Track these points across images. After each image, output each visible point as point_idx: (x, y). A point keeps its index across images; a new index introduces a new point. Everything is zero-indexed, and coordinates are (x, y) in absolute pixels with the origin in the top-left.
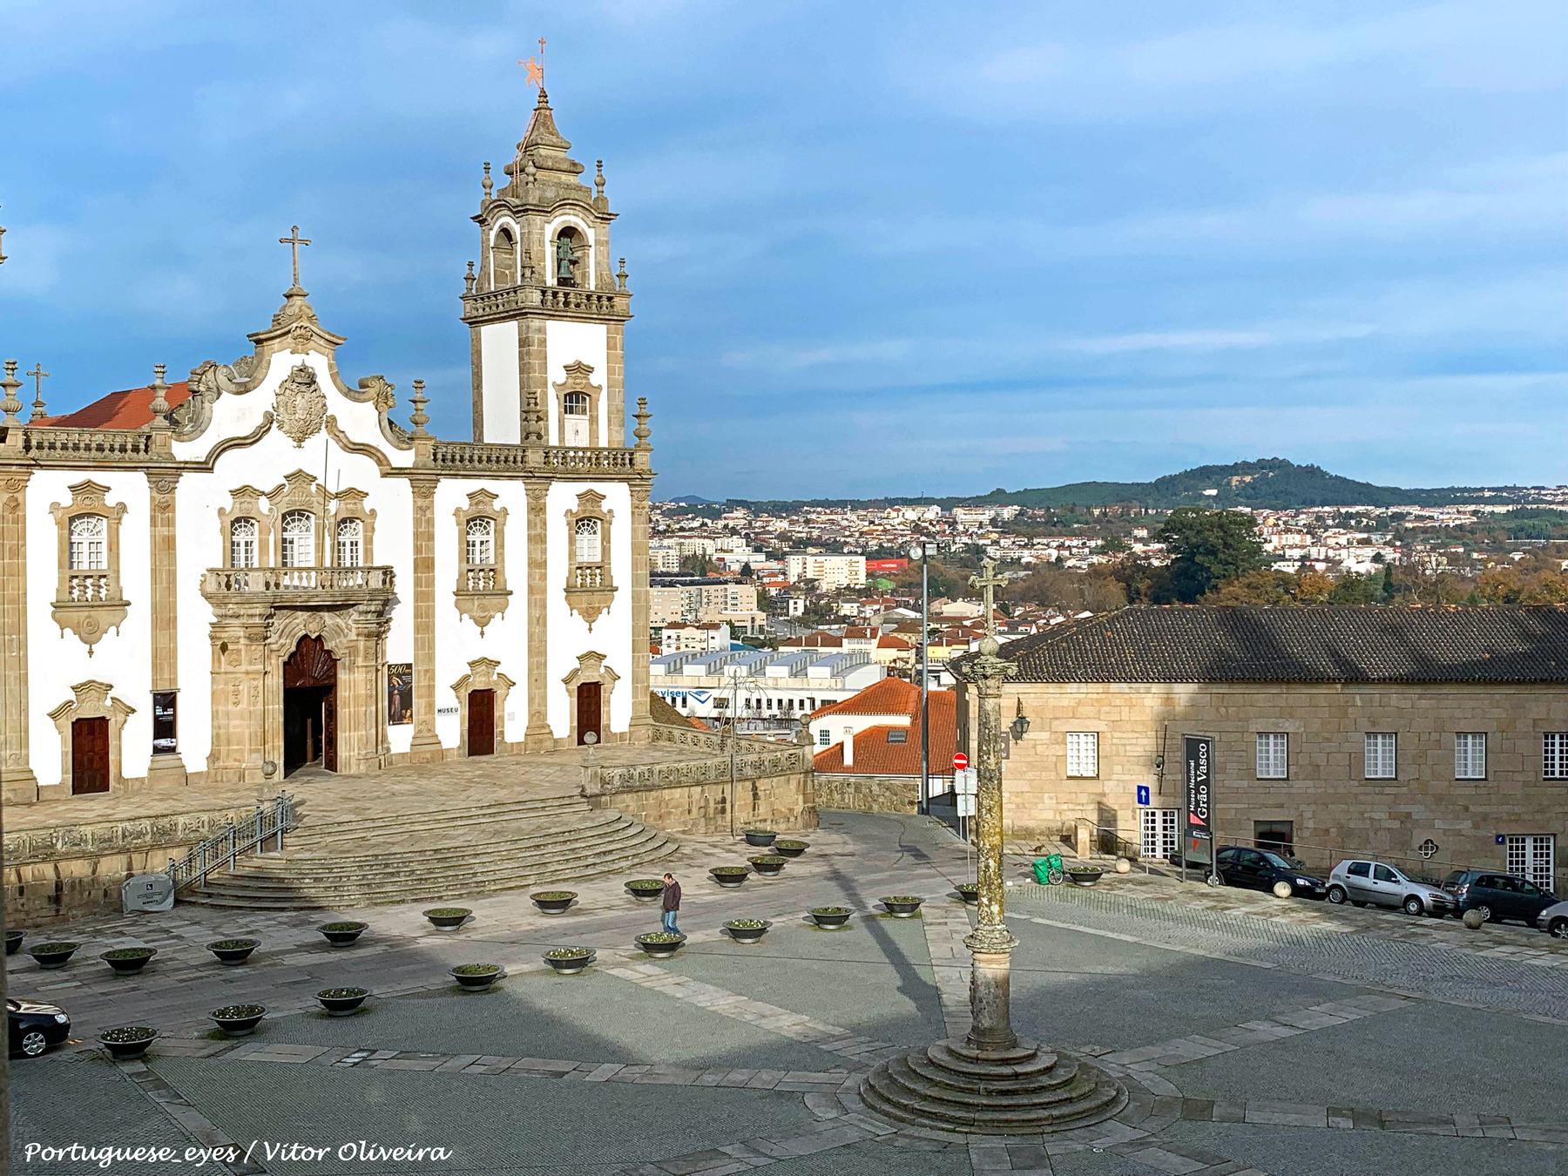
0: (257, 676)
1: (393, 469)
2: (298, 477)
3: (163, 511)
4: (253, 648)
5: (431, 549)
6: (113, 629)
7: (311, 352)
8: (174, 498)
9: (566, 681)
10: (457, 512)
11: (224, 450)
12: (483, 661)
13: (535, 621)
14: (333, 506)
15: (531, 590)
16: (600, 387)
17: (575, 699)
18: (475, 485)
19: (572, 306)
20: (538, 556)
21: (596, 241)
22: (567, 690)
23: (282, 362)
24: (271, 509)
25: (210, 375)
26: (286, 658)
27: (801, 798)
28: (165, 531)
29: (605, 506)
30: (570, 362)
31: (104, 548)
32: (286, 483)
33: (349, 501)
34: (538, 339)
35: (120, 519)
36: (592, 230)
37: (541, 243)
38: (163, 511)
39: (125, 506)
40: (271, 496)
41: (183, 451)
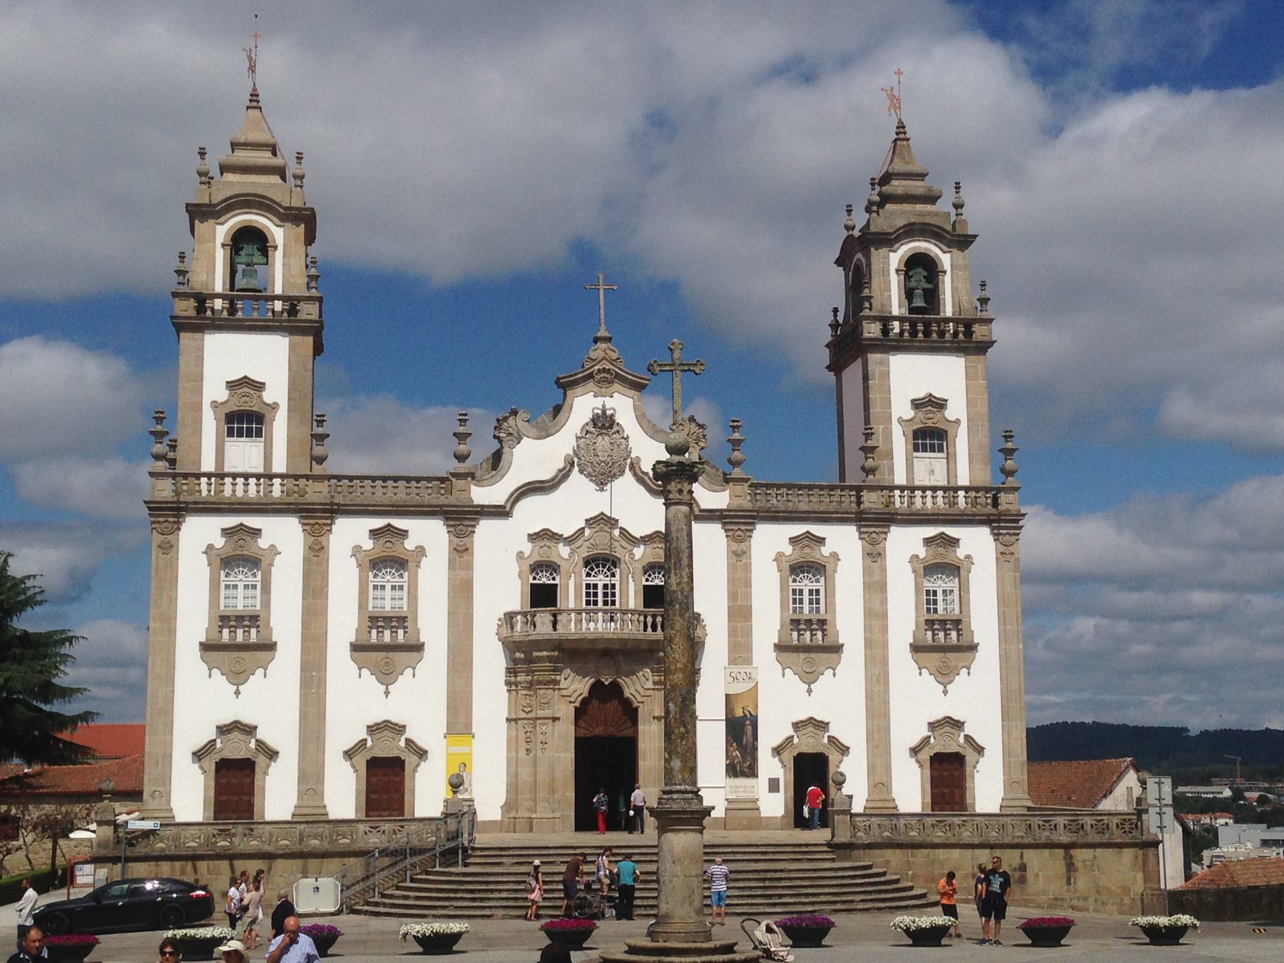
0: (546, 721)
2: (603, 521)
3: (461, 553)
5: (748, 596)
6: (409, 671)
7: (616, 395)
8: (472, 542)
9: (915, 751)
10: (779, 557)
12: (811, 721)
13: (874, 679)
14: (639, 552)
15: (868, 644)
16: (958, 422)
17: (928, 772)
18: (798, 529)
19: (934, 335)
20: (877, 607)
21: (952, 265)
22: (918, 761)
23: (584, 406)
24: (571, 554)
25: (511, 421)
26: (577, 704)
27: (1140, 876)
28: (463, 574)
29: (961, 553)
30: (920, 394)
31: (405, 593)
33: (655, 546)
34: (879, 372)
35: (419, 562)
36: (948, 255)
37: (886, 273)
38: (461, 553)
39: (424, 549)
40: (569, 540)
41: (481, 495)
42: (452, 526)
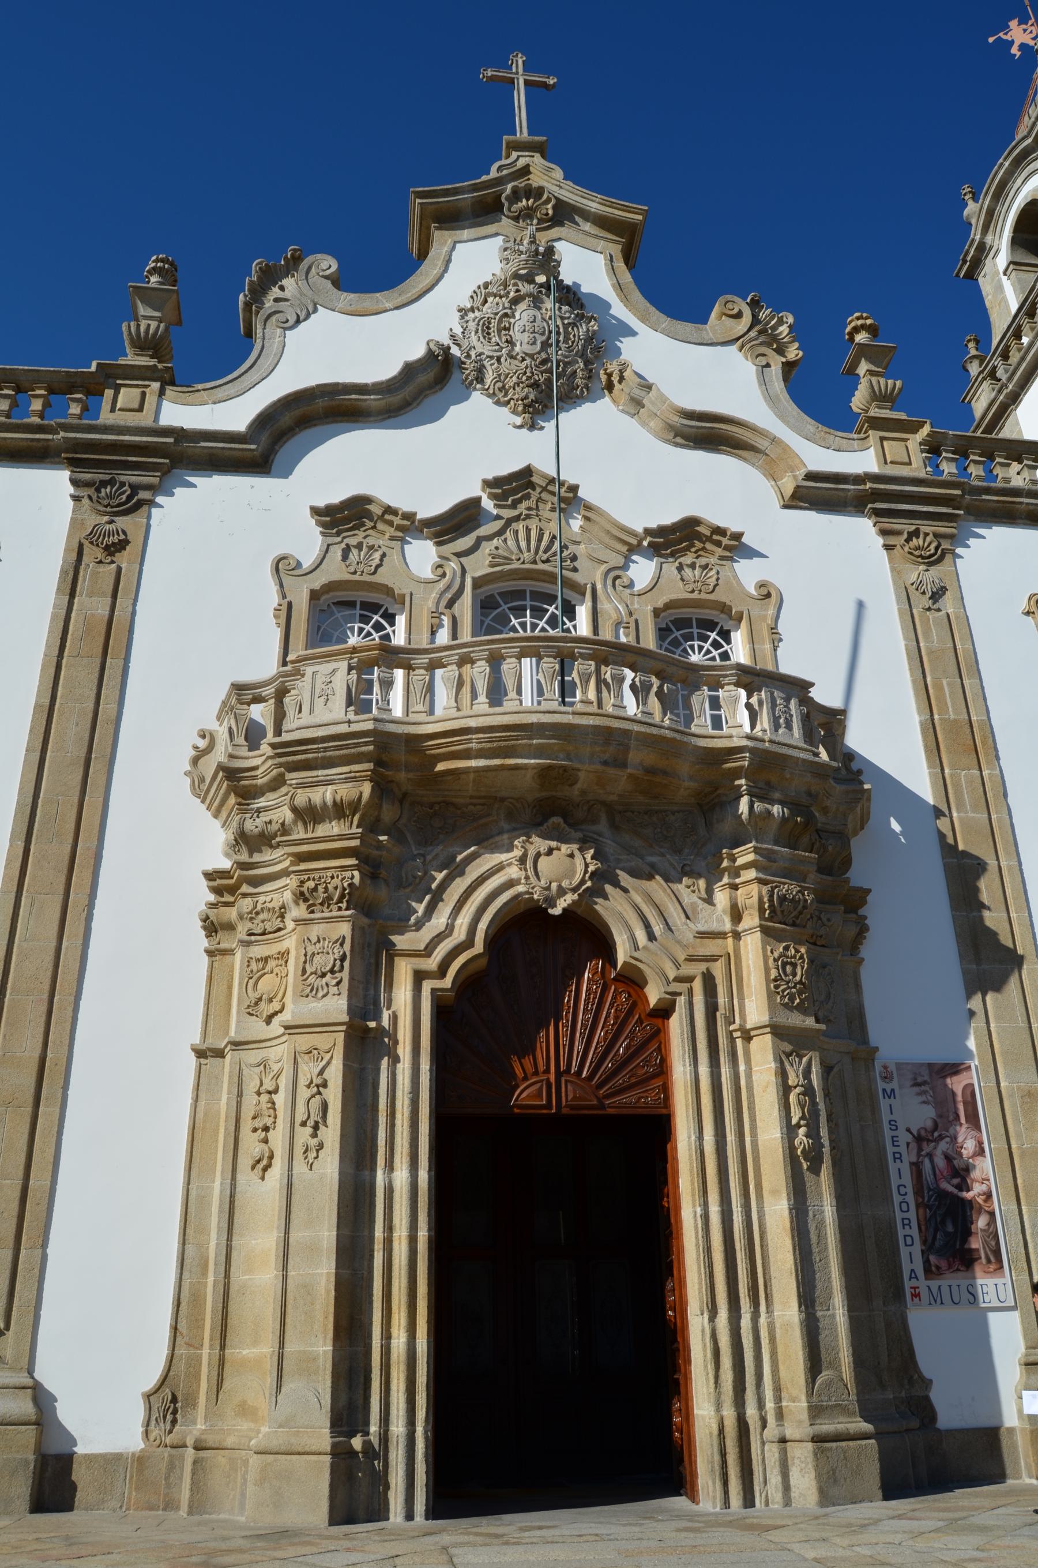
0: (322, 1041)
1: (811, 476)
4: (316, 931)
11: (305, 422)
26: (447, 982)
32: (488, 504)
42: (88, 484)
